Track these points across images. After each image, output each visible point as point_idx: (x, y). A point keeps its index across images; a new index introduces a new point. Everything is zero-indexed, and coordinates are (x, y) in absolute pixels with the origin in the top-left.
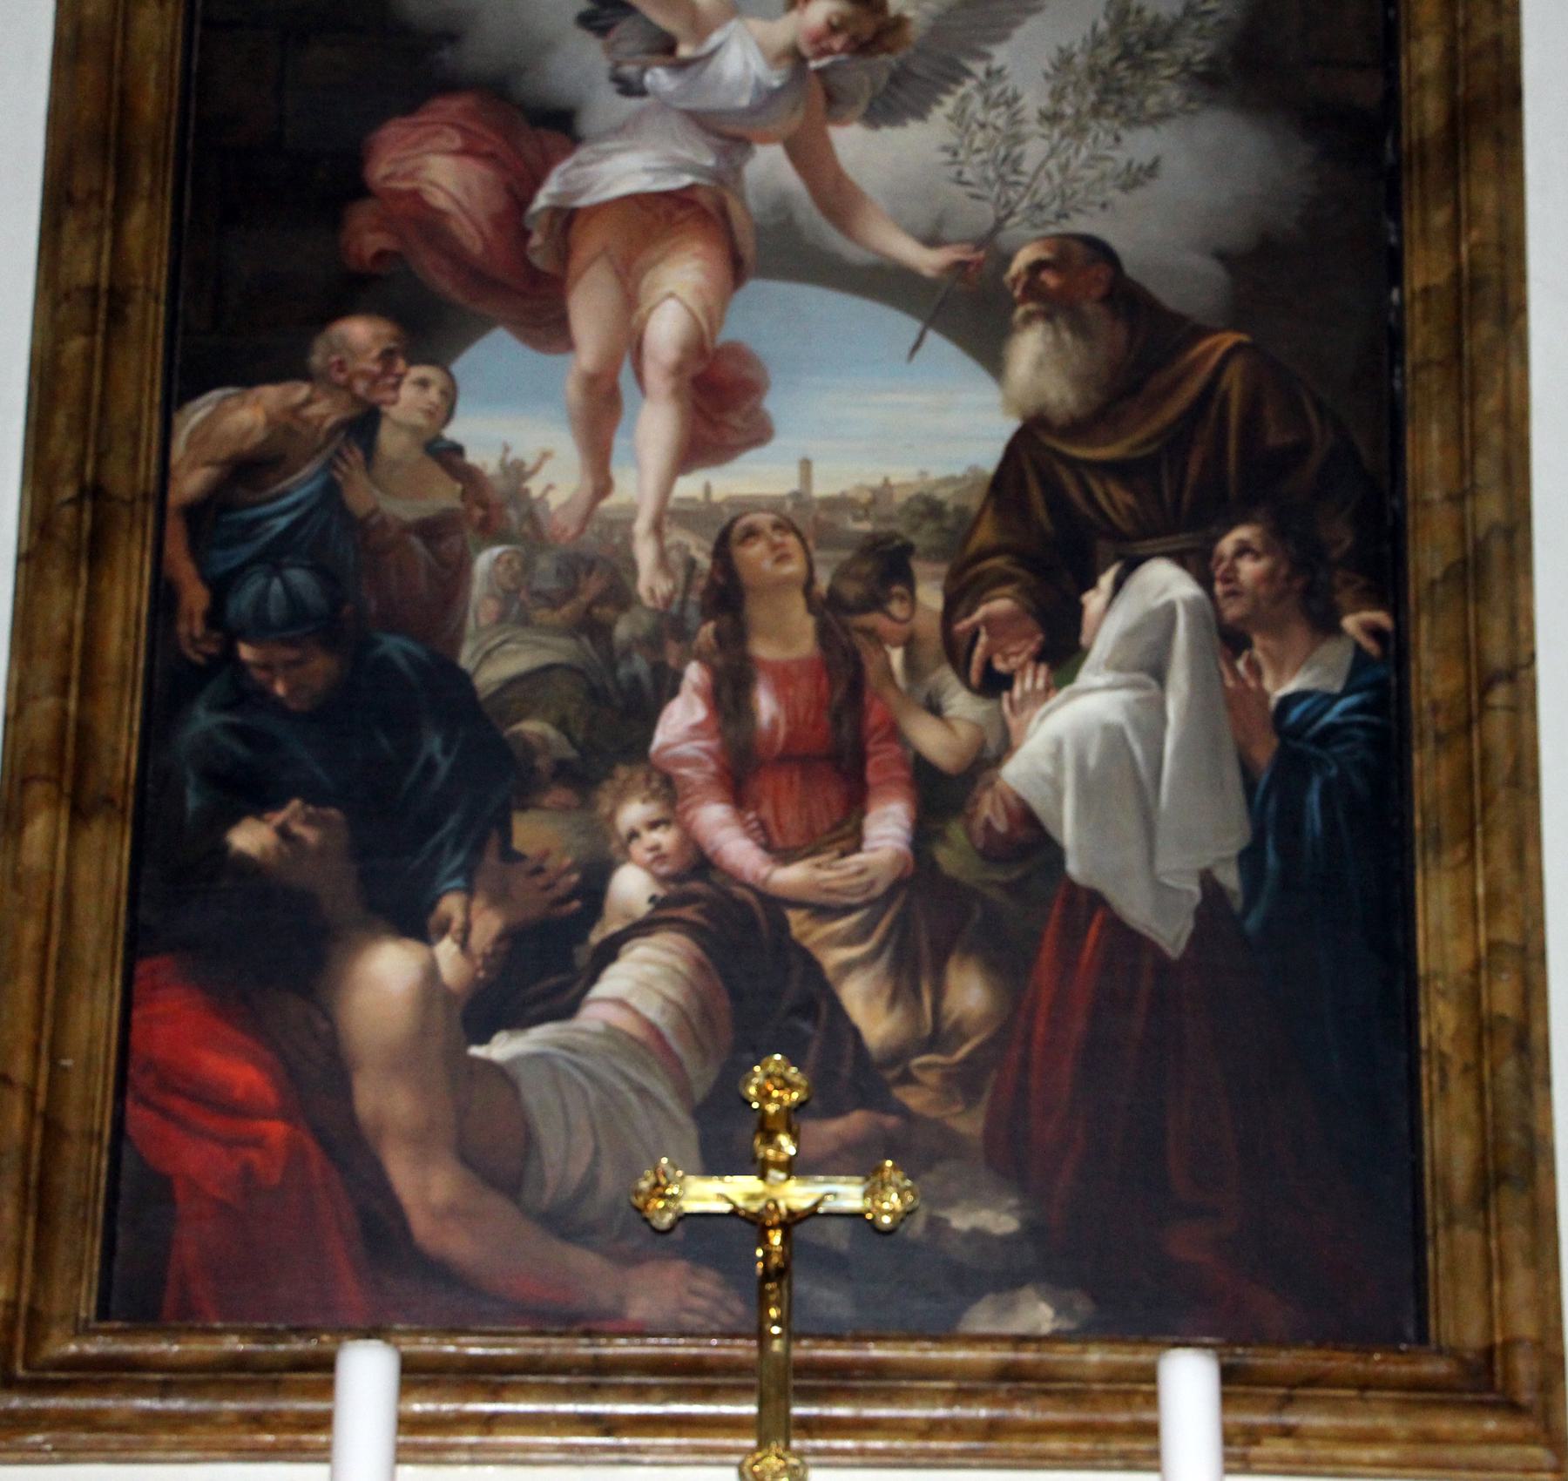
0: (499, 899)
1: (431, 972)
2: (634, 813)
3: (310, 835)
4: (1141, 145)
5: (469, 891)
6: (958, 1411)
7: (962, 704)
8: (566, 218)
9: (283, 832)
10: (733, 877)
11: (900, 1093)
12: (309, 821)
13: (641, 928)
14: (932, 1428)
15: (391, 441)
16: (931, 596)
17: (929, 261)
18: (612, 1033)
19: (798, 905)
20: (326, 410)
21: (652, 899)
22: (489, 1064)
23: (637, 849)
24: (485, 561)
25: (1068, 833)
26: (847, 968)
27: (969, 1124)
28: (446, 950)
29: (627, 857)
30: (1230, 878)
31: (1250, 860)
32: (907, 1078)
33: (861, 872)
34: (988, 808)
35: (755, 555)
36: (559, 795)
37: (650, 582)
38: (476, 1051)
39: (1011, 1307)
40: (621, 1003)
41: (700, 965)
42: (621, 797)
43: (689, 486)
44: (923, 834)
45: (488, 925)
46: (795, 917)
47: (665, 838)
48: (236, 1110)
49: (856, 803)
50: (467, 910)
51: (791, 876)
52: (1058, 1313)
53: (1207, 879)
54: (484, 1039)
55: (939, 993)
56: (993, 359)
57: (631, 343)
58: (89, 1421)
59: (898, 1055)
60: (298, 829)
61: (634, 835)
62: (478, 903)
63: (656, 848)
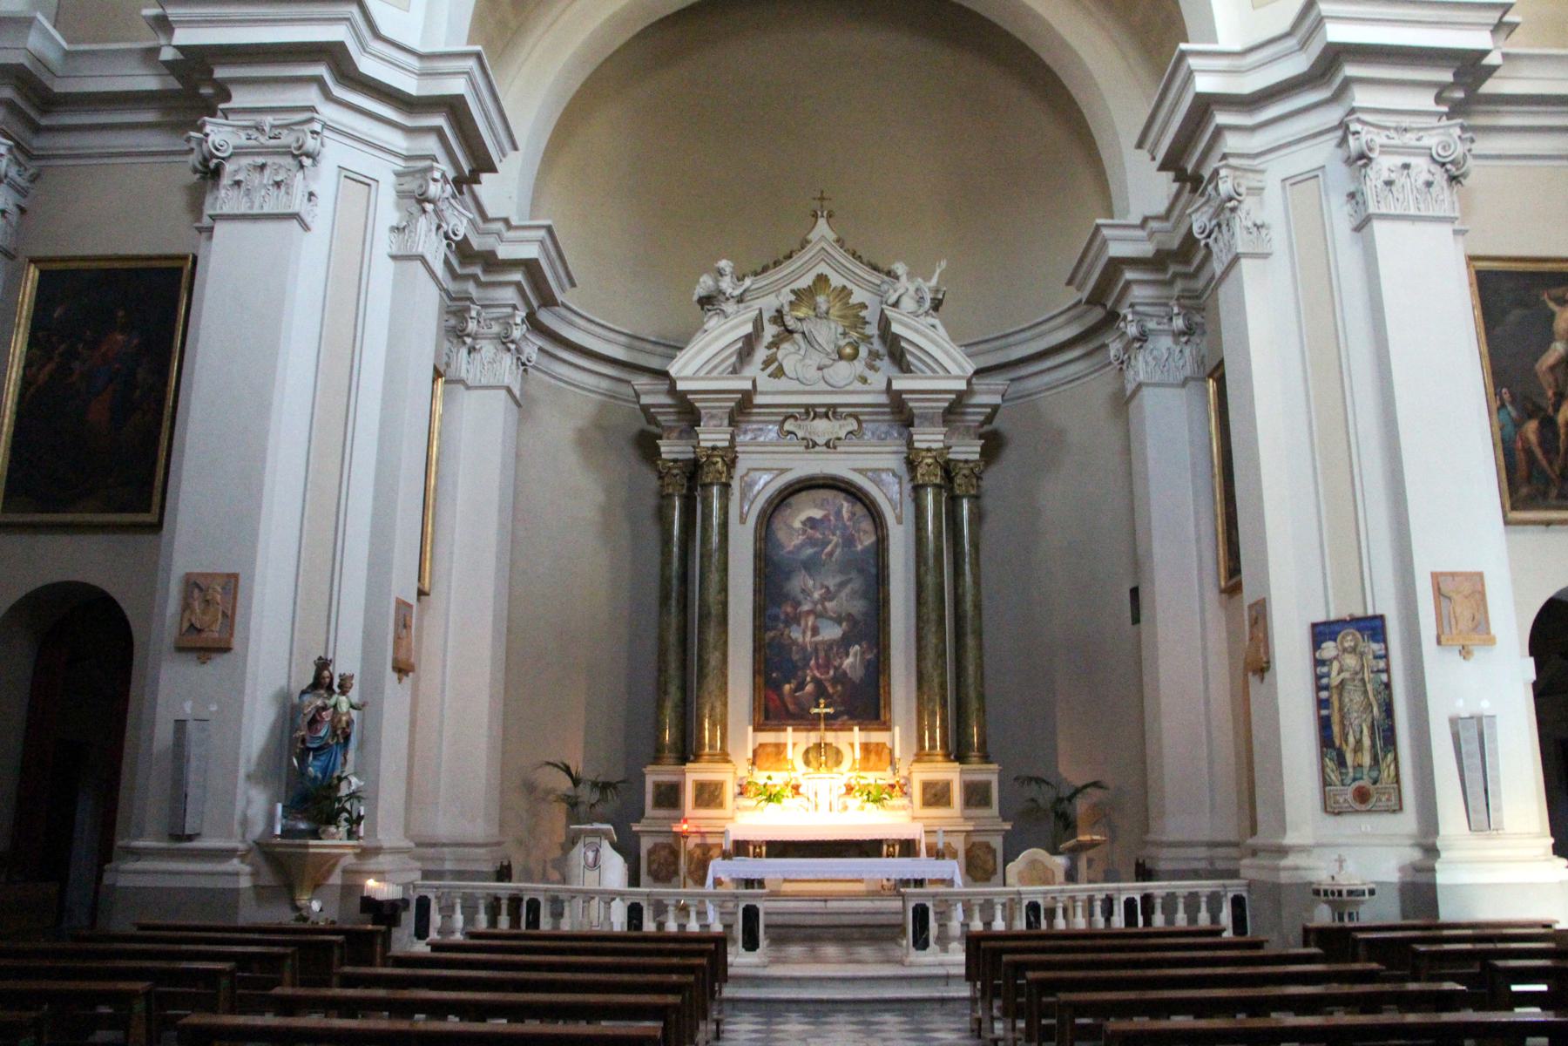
4: (855, 603)
7: (839, 660)
8: (800, 613)
15: (785, 636)
16: (835, 649)
17: (835, 616)
20: (779, 633)
24: (794, 648)
25: (848, 671)
27: (839, 700)
34: (841, 671)
35: (820, 647)
37: (809, 649)
43: (813, 639)
49: (829, 669)
56: (840, 624)
57: (807, 624)
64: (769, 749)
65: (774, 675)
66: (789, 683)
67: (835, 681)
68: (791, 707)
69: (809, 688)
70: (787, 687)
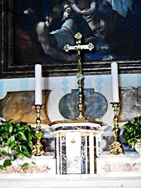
0: (52, 17)
1: (45, 25)
2: (66, 6)
3: (32, 11)
5: (49, 16)
6: (101, 69)
9: (29, 11)
10: (77, 12)
11: (96, 35)
12: (32, 10)
13: (67, 19)
14: (98, 71)
18: (64, 30)
19: (83, 15)
21: (68, 15)
22: (52, 34)
23: (66, 10)
26: (89, 21)
27: (103, 37)
28: (47, 22)
29: (65, 11)
30: (131, 8)
31: (133, 6)
32: (96, 33)
33: (90, 11)
36: (58, 5)
38: (50, 33)
39: (108, 57)
40: (65, 27)
41: (73, 22)
42: (64, 4)
44: (97, 6)
45: (51, 20)
46: (83, 16)
47: (69, 9)
48: (26, 41)
50: (49, 18)
51: (83, 12)
52: (113, 57)
53: (128, 9)
54: (51, 32)
55: (99, 23)
58: (13, 74)
59: (95, 30)
60: (31, 11)
61: (66, 8)
62: (50, 17)
63: (68, 10)
64: (19, 99)
65: (26, 12)
66: (44, 21)
67: (96, 16)
68: (46, 48)
69: (67, 24)
70: (41, 25)
